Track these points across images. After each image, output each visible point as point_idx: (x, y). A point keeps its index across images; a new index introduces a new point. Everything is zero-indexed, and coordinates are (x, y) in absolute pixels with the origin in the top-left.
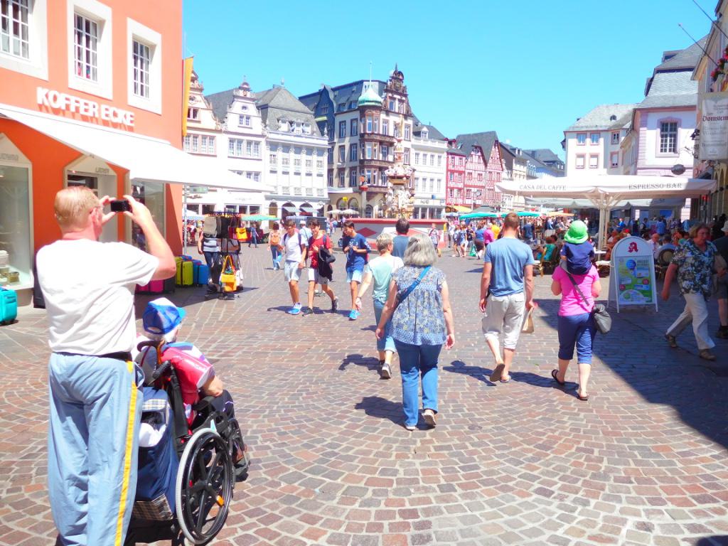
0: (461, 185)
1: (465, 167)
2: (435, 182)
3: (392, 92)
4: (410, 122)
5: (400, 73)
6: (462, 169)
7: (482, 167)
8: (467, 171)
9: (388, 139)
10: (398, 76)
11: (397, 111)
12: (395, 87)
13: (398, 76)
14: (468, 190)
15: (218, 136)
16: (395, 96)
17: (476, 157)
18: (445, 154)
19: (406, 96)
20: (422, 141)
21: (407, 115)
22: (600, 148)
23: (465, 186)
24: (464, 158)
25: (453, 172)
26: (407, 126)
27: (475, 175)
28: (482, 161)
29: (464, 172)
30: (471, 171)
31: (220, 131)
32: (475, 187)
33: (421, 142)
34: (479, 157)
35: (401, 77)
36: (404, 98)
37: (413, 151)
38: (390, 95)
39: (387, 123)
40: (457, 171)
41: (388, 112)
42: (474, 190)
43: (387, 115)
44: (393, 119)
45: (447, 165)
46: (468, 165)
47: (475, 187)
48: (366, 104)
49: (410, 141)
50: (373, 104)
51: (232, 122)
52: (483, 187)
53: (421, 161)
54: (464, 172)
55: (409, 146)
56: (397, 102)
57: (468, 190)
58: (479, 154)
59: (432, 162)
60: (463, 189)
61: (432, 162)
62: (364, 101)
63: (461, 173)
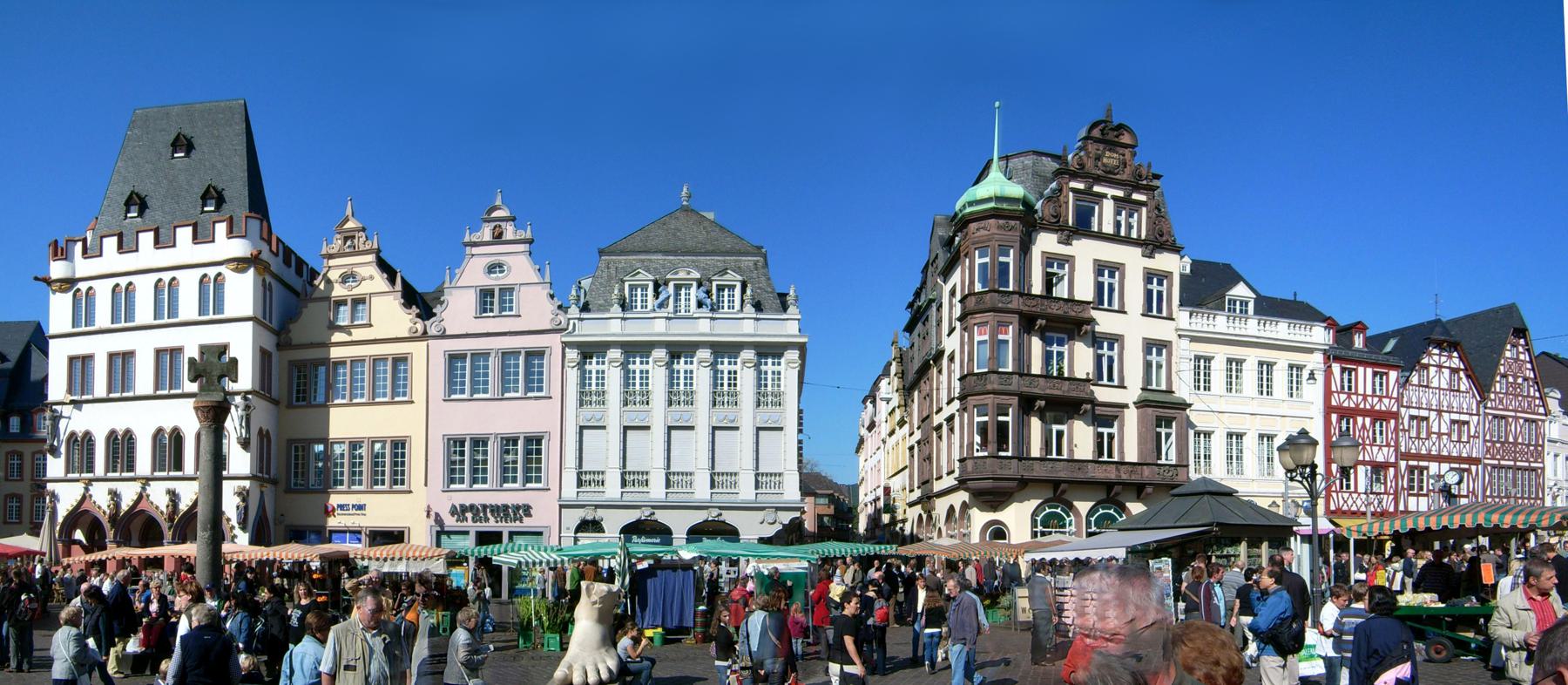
1: (1399, 400)
4: (1168, 262)
11: (1108, 228)
14: (1411, 470)
15: (417, 350)
17: (1441, 368)
21: (1155, 243)
23: (1407, 456)
24: (1393, 375)
25: (1347, 414)
28: (1465, 384)
29: (1396, 416)
30: (1424, 413)
31: (425, 335)
32: (1440, 459)
33: (1220, 324)
37: (1184, 352)
40: (1365, 413)
42: (1434, 467)
45: (1328, 393)
46: (1412, 395)
47: (1449, 459)
49: (1170, 318)
51: (458, 310)
52: (1476, 461)
54: (1396, 416)
57: (1411, 470)
59: (1265, 387)
60: (1395, 465)
61: (1265, 387)
63: (1379, 417)
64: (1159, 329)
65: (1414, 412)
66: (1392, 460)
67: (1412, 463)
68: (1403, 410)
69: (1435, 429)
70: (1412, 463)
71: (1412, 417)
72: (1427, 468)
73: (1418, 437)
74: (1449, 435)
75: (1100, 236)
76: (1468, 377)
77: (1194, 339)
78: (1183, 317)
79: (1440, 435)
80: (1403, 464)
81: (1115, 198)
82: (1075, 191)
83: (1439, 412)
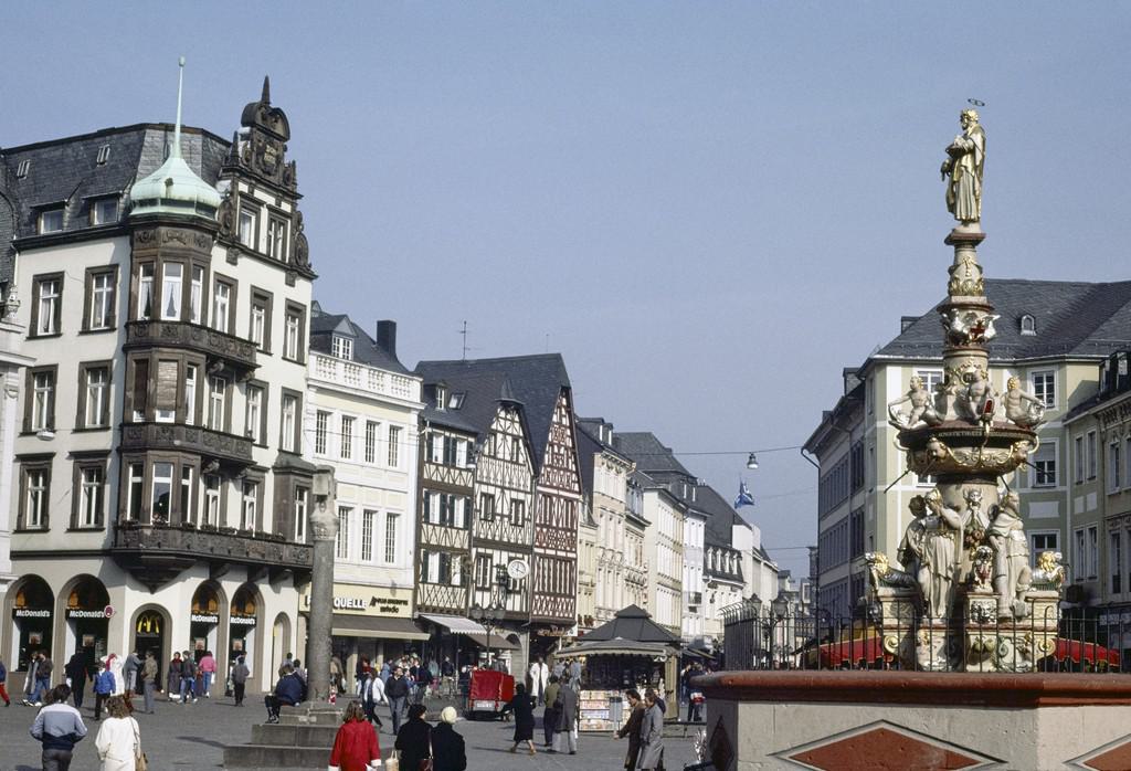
0: (459, 540)
2: (379, 522)
3: (245, 174)
4: (303, 292)
5: (278, 114)
6: (464, 480)
7: (523, 476)
8: (480, 489)
9: (233, 352)
10: (265, 120)
12: (256, 153)
13: (265, 120)
14: (479, 556)
16: (258, 194)
18: (413, 418)
19: (294, 197)
20: (340, 366)
21: (297, 268)
22: (898, 431)
23: (478, 542)
26: (294, 310)
27: (503, 506)
30: (491, 490)
34: (515, 439)
35: (279, 129)
36: (286, 207)
37: (312, 401)
38: (243, 187)
39: (242, 289)
41: (236, 249)
42: (500, 557)
43: (232, 261)
44: (250, 273)
48: (160, 209)
49: (300, 362)
50: (191, 212)
53: (334, 442)
55: (300, 386)
56: (264, 212)
57: (479, 556)
58: (517, 430)
62: (144, 203)
64: (293, 377)
65: (484, 489)
66: (466, 547)
67: (481, 550)
68: (477, 485)
69: (499, 511)
70: (481, 550)
71: (483, 494)
72: (491, 557)
73: (486, 520)
74: (510, 517)
75: (254, 254)
76: (526, 445)
77: (321, 390)
78: (312, 359)
79: (502, 516)
80: (474, 551)
81: (270, 208)
82: (242, 194)
83: (503, 488)
